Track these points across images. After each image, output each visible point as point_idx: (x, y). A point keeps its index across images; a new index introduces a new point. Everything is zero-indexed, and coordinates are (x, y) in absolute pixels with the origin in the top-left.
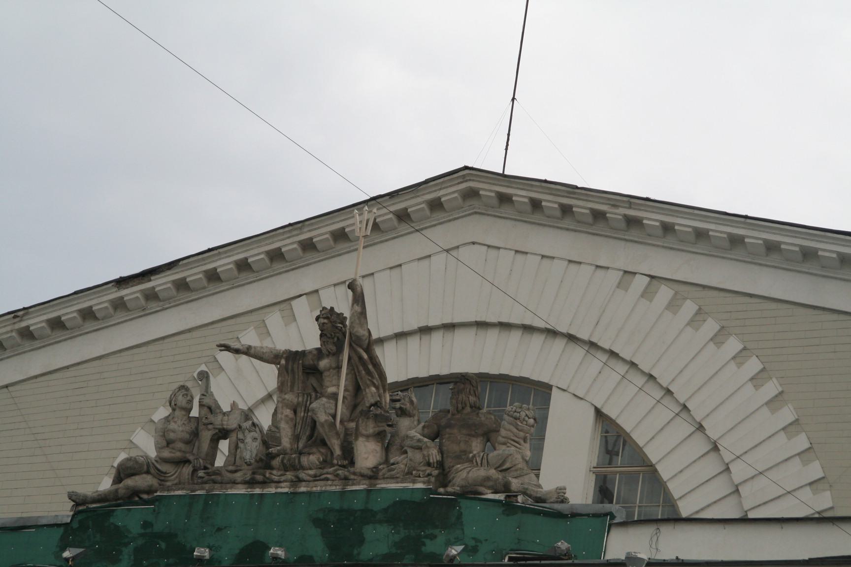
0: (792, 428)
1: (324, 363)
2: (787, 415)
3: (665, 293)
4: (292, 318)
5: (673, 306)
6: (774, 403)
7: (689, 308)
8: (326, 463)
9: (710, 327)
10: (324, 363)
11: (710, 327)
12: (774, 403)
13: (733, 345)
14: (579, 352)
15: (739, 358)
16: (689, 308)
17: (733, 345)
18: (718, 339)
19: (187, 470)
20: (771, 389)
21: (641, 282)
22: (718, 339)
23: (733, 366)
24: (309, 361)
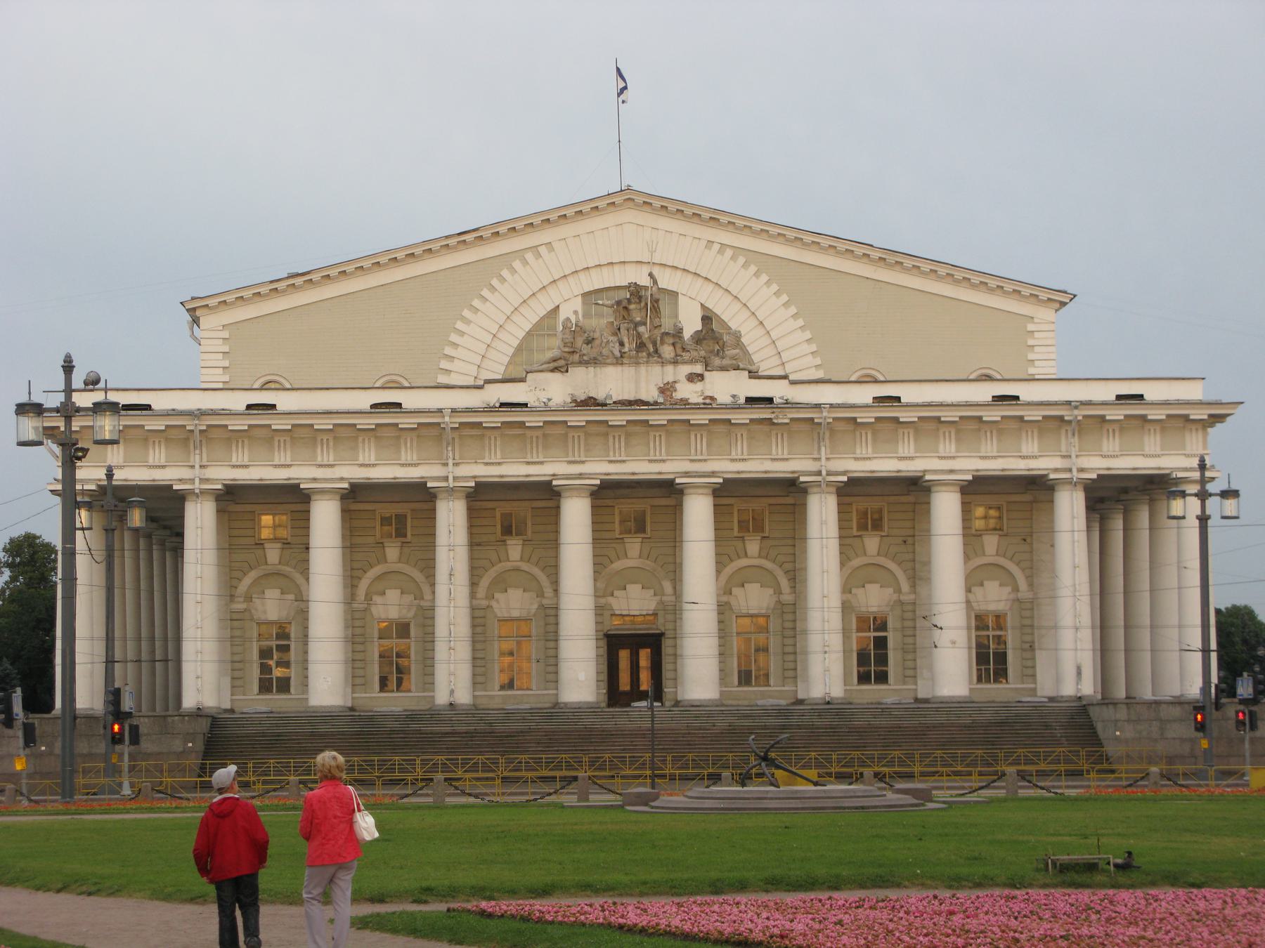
0: (795, 316)
1: (632, 307)
2: (793, 310)
3: (729, 253)
4: (538, 256)
5: (733, 258)
6: (786, 305)
7: (741, 260)
8: (649, 355)
9: (753, 269)
10: (632, 307)
11: (753, 269)
12: (786, 305)
13: (764, 278)
14: (690, 277)
15: (768, 283)
16: (741, 260)
17: (764, 278)
18: (757, 275)
19: (576, 357)
20: (785, 298)
21: (716, 247)
22: (757, 275)
23: (765, 288)
24: (625, 303)
